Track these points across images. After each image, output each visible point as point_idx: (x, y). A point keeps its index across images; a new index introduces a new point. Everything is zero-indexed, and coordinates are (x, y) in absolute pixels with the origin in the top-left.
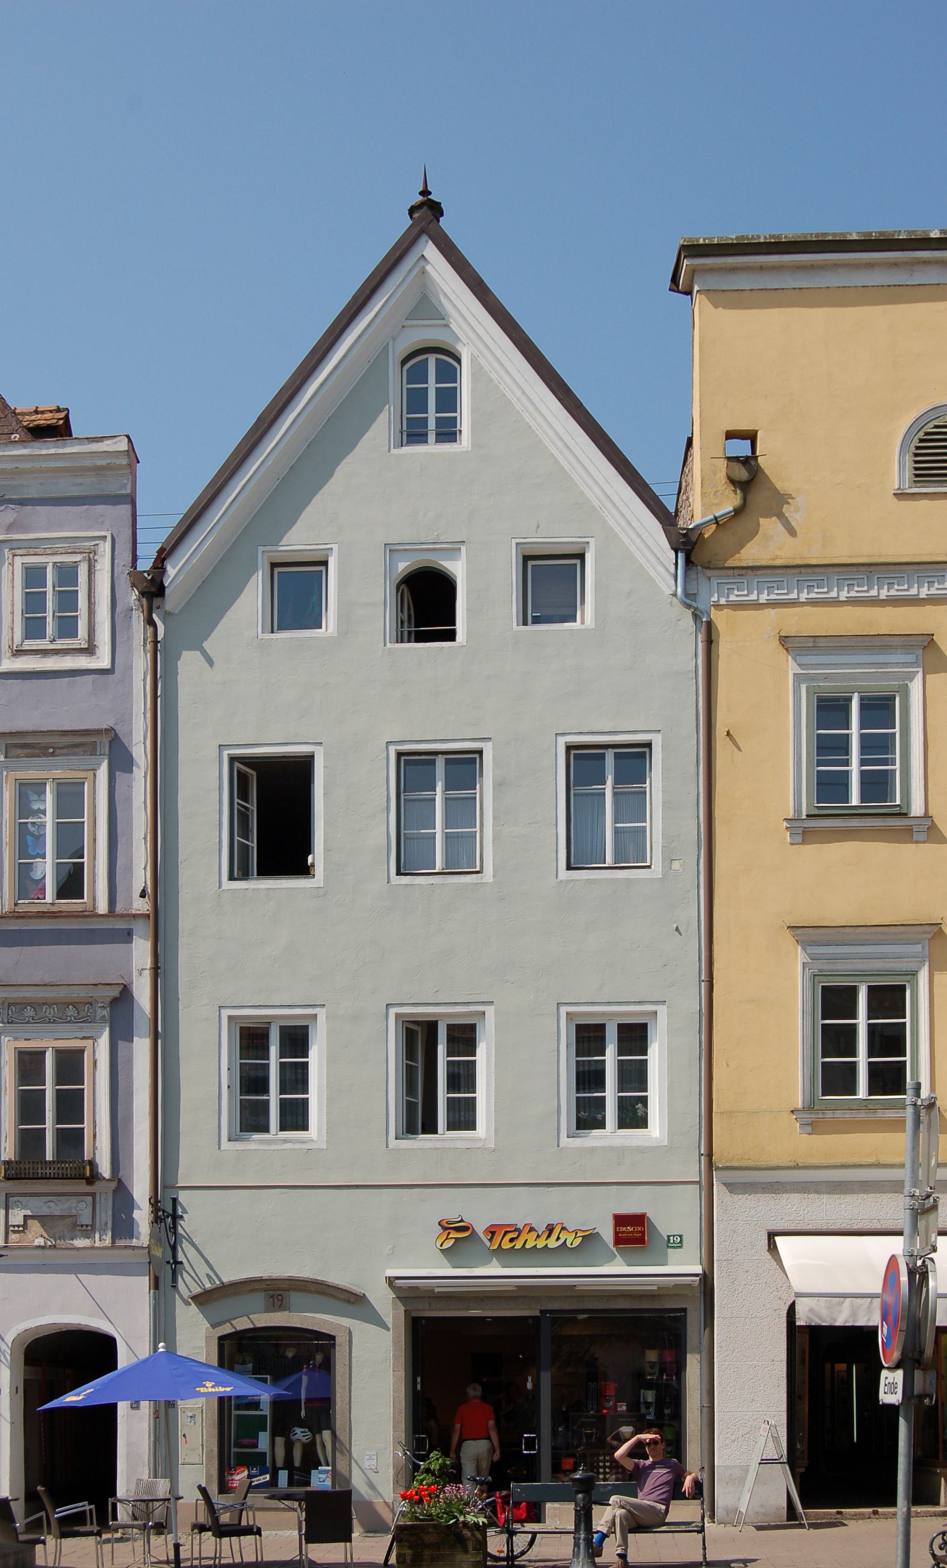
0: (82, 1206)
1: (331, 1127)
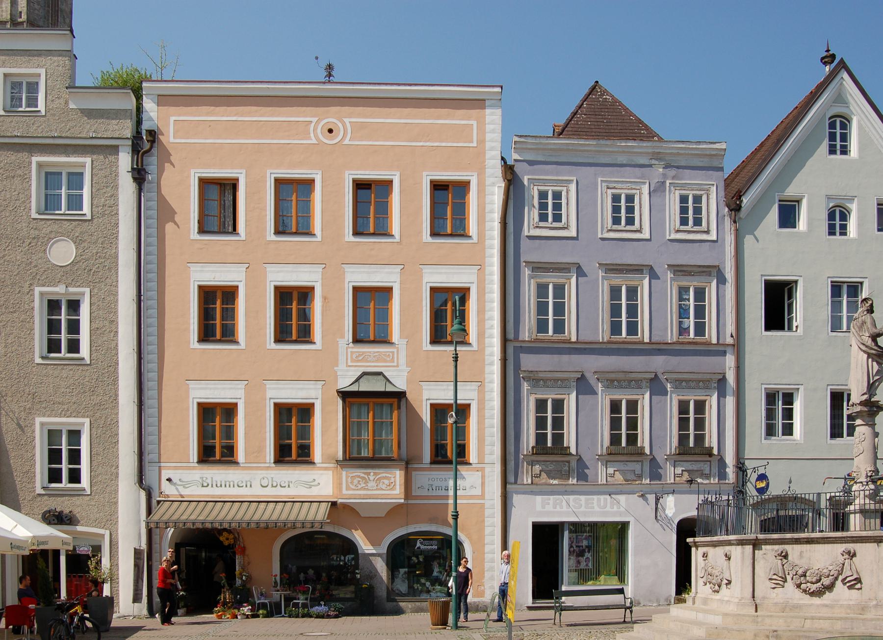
0: (706, 466)
1: (806, 433)
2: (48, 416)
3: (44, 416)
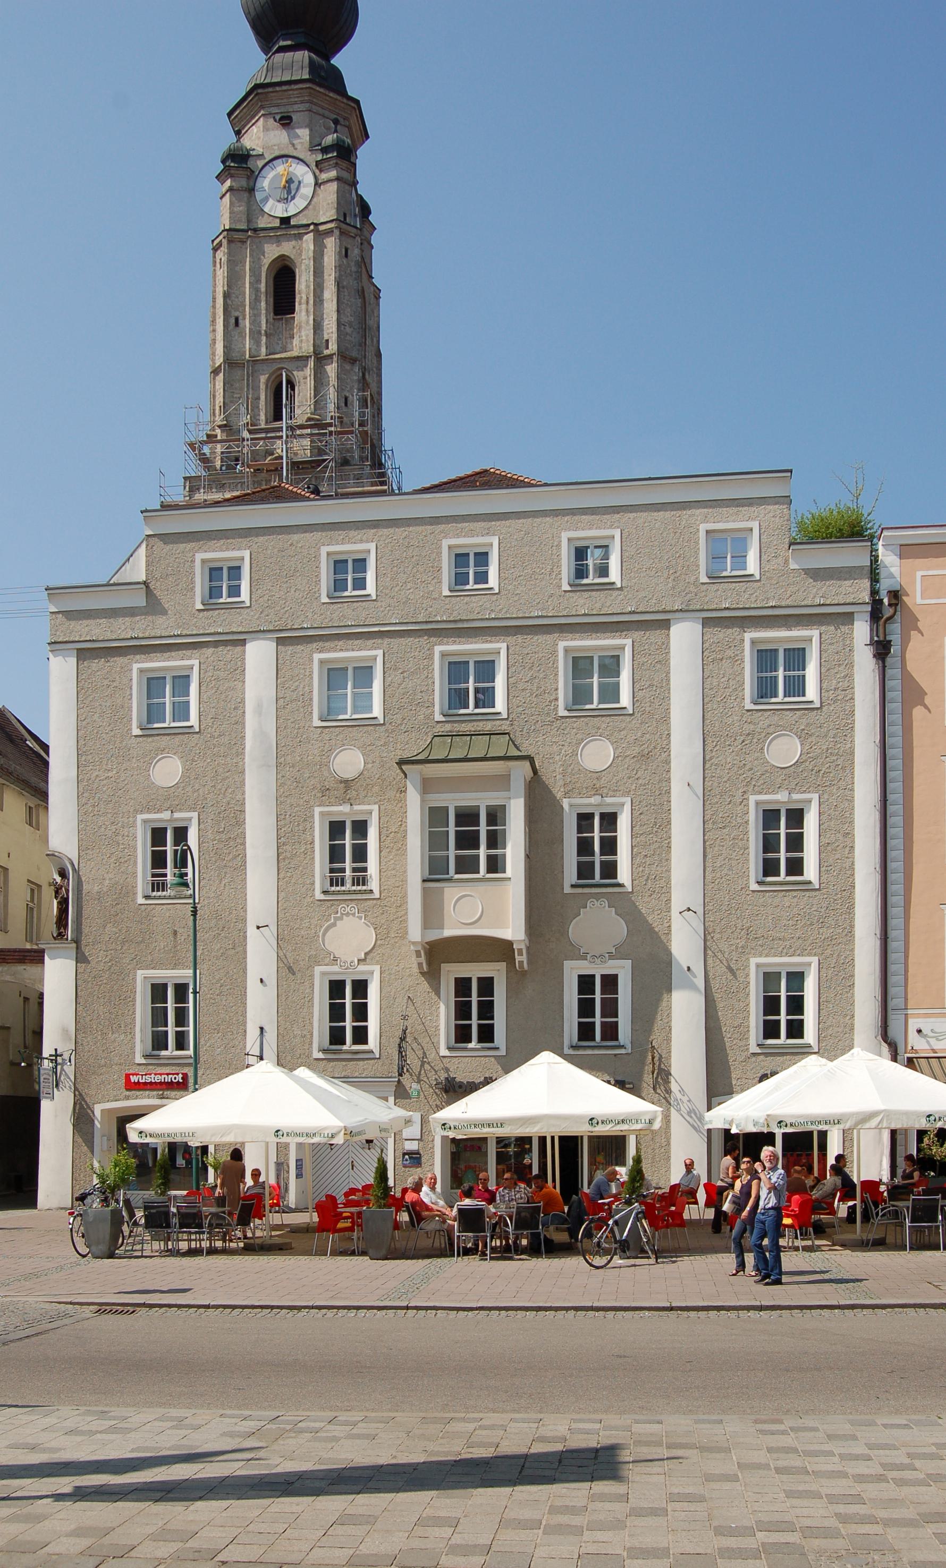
2: (766, 956)
3: (761, 956)
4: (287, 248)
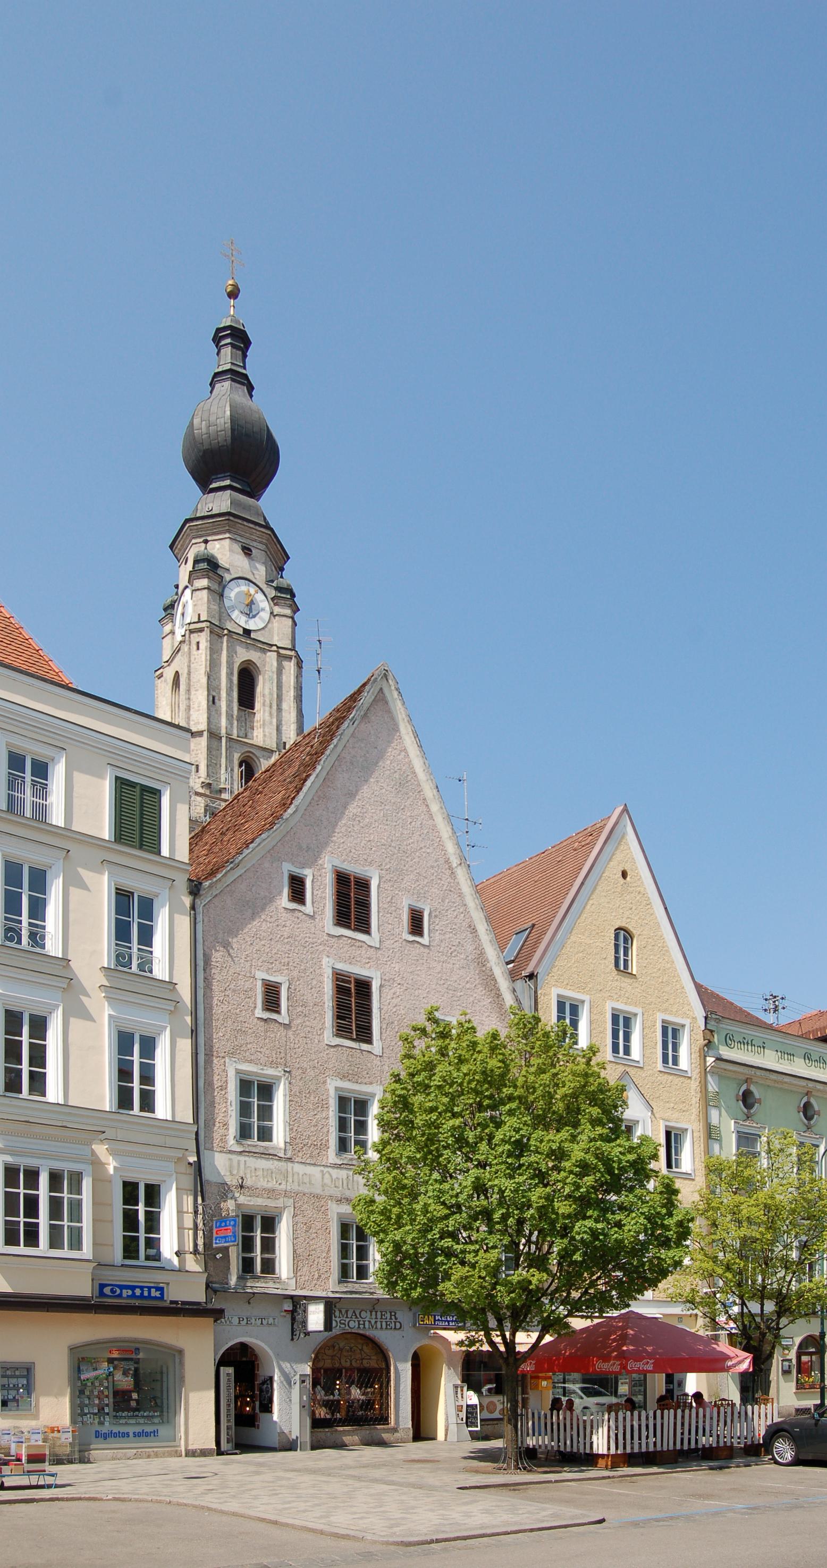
4: (254, 656)
